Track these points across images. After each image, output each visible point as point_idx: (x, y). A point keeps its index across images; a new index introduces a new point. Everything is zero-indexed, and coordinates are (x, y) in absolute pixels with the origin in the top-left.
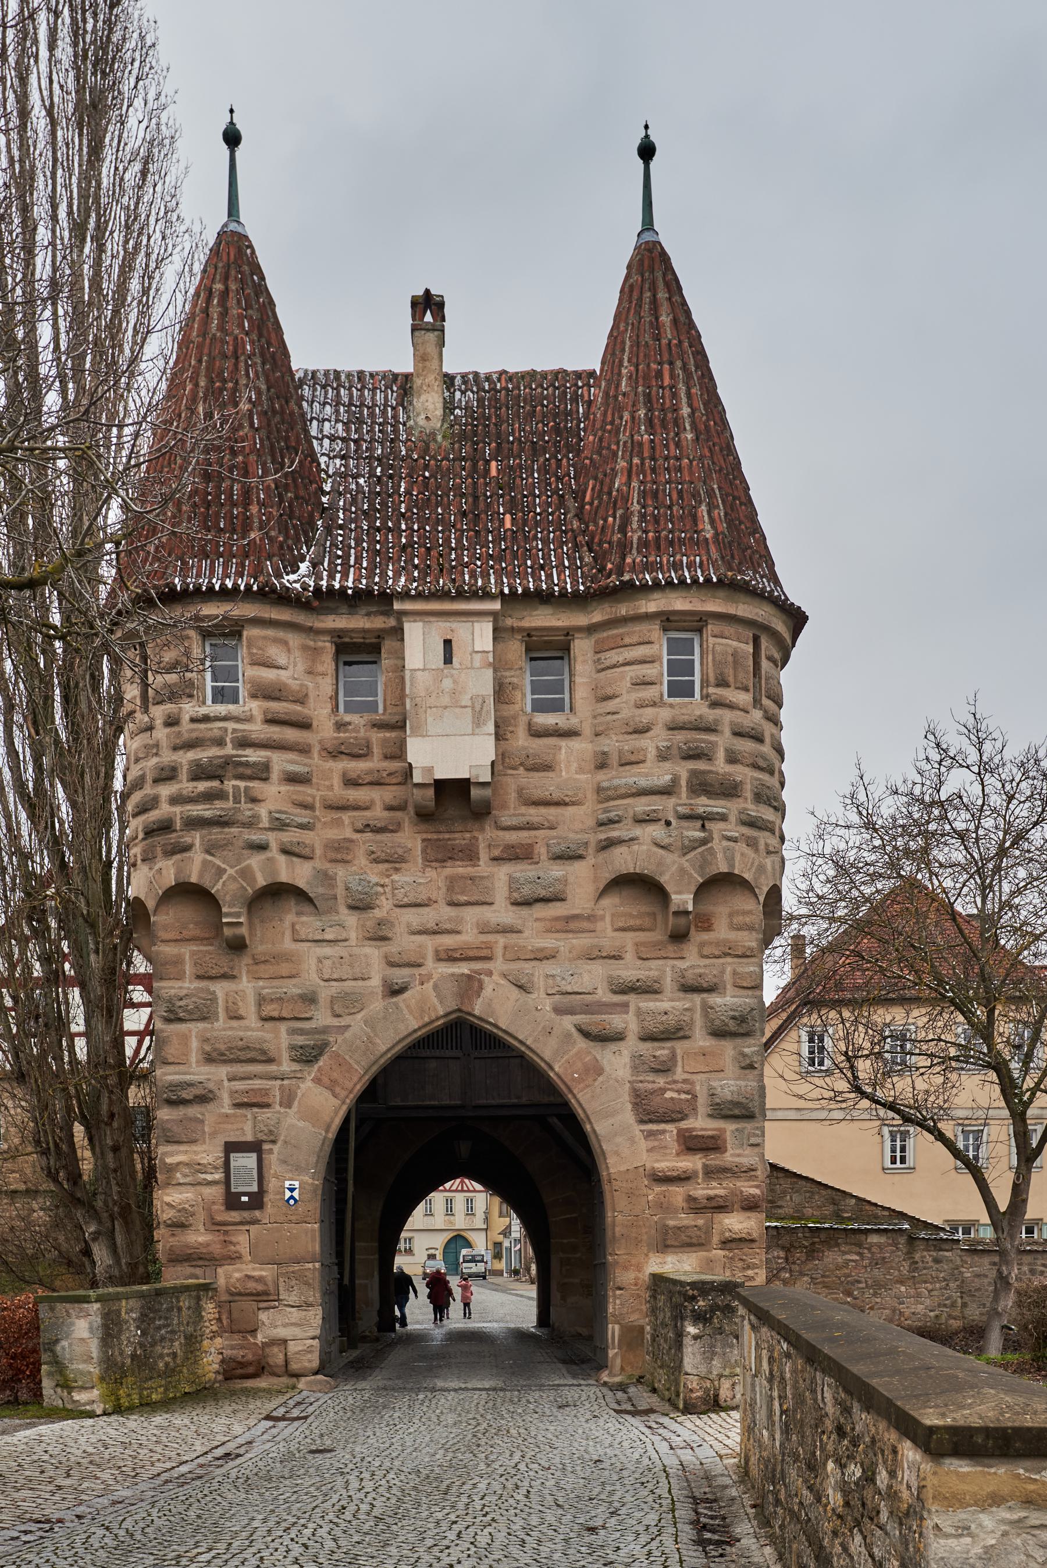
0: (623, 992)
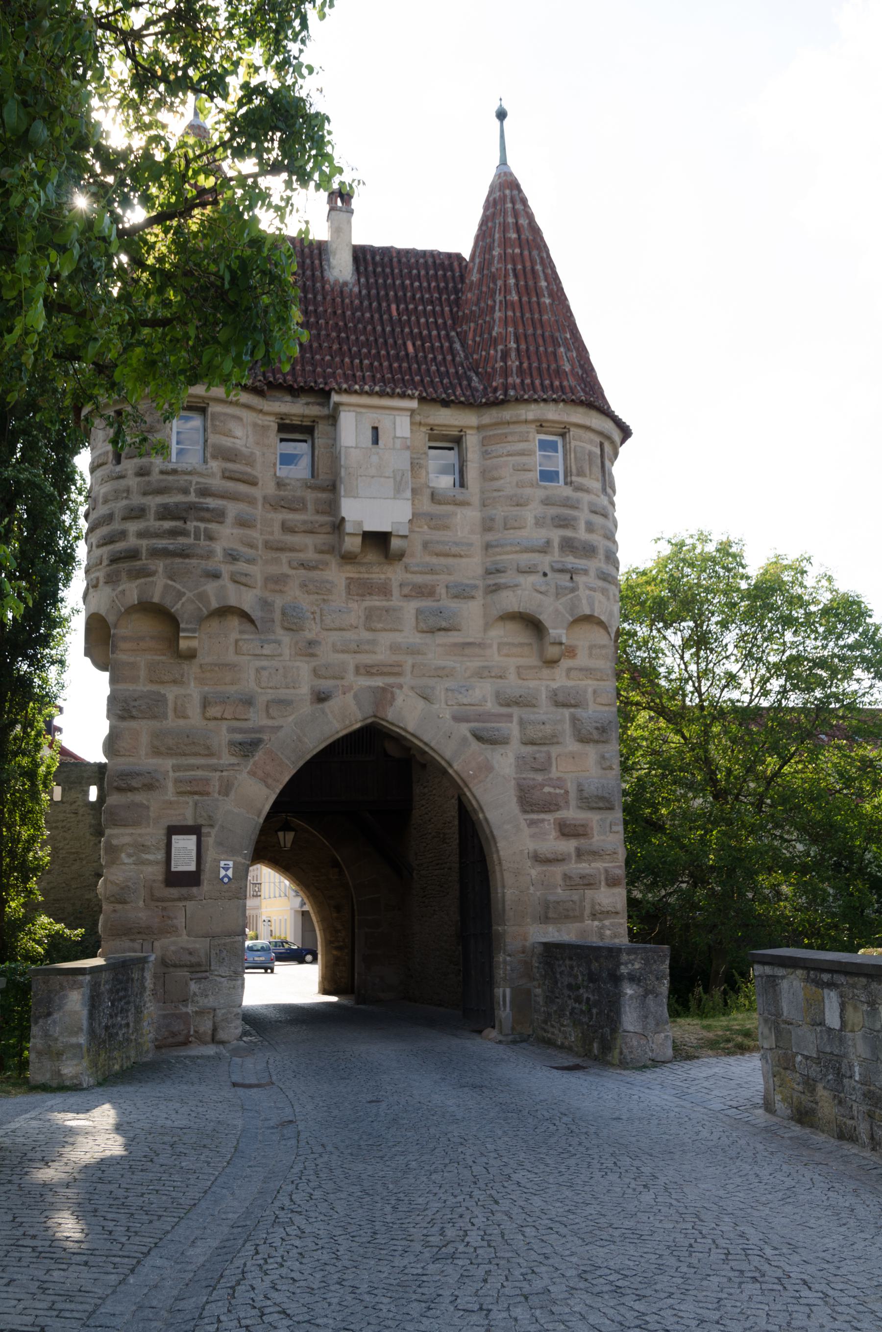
0: (508, 705)
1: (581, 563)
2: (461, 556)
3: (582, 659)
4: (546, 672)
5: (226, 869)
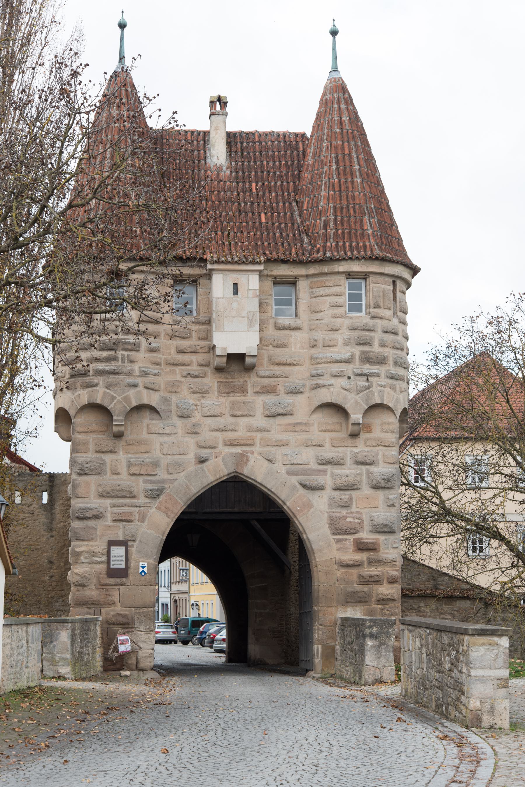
0: (324, 464)
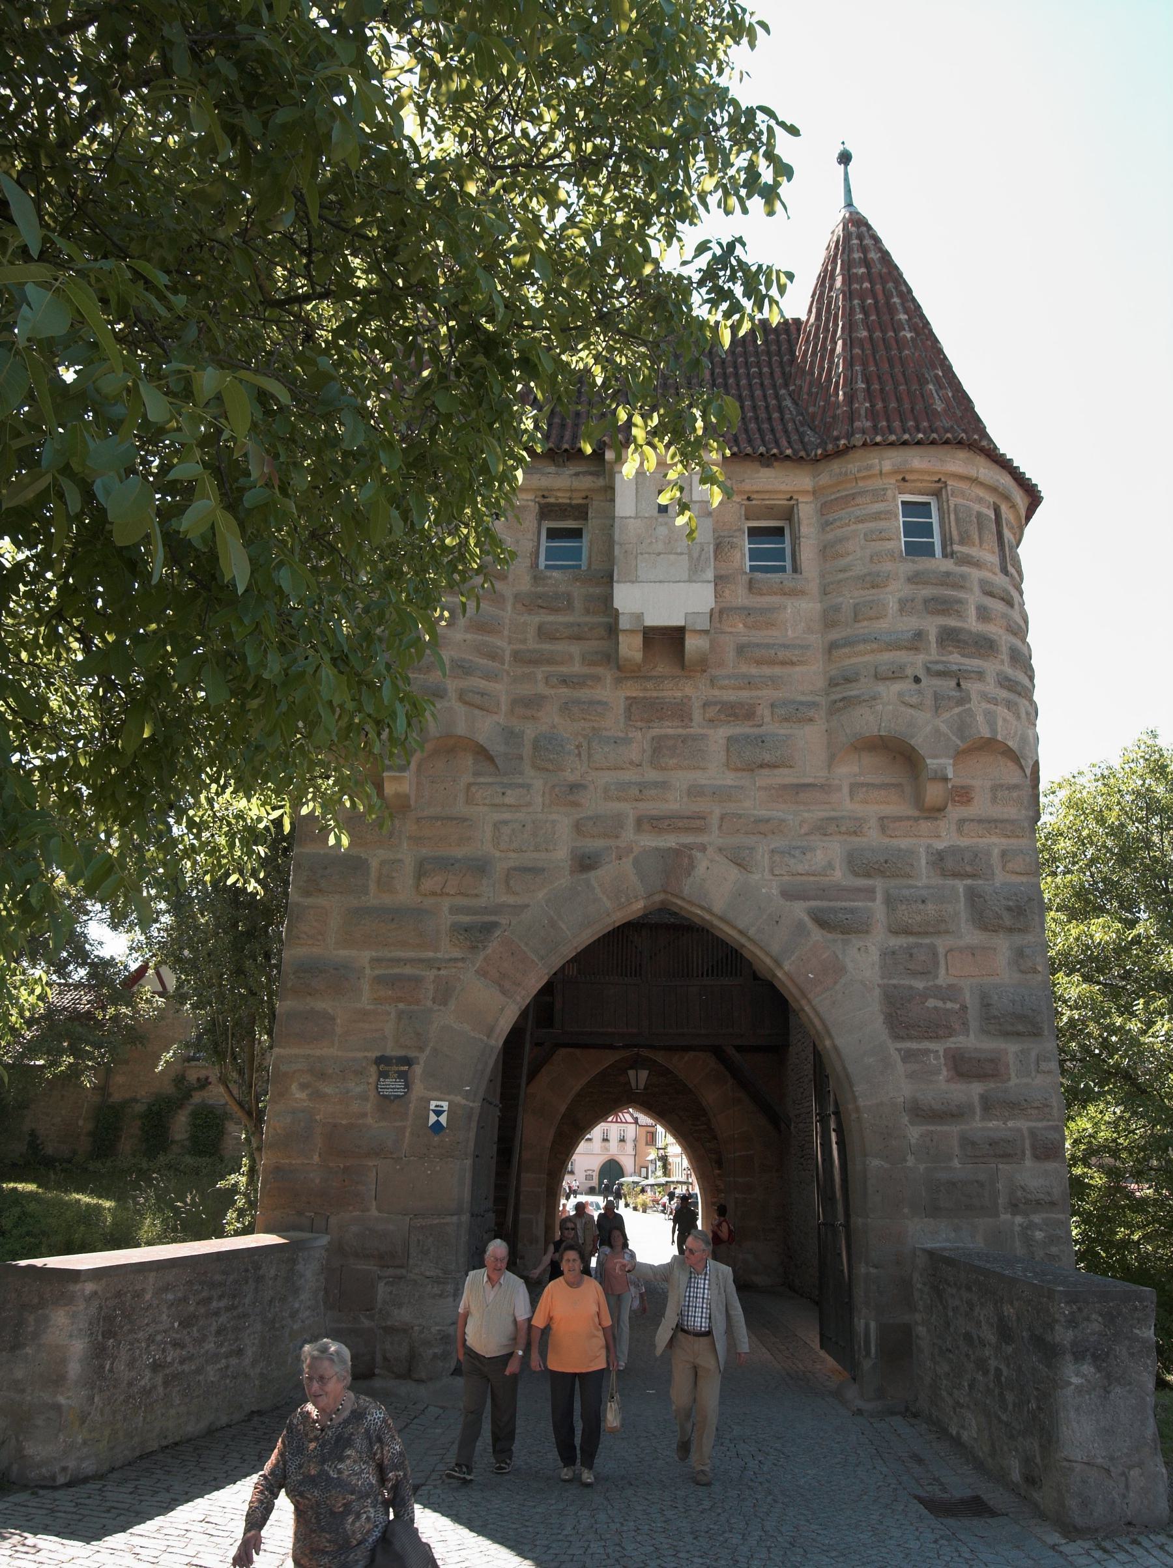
0: (868, 875)
1: (974, 663)
2: (793, 663)
3: (981, 806)
4: (925, 826)
5: (438, 1113)
